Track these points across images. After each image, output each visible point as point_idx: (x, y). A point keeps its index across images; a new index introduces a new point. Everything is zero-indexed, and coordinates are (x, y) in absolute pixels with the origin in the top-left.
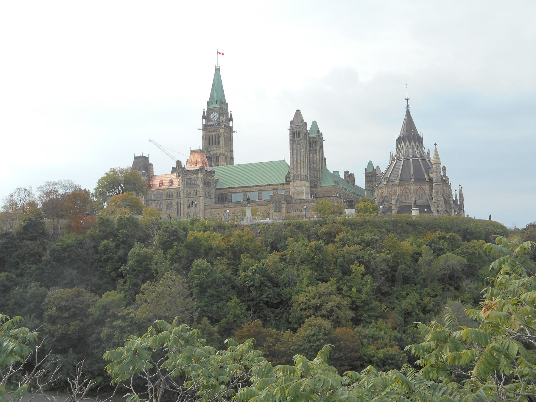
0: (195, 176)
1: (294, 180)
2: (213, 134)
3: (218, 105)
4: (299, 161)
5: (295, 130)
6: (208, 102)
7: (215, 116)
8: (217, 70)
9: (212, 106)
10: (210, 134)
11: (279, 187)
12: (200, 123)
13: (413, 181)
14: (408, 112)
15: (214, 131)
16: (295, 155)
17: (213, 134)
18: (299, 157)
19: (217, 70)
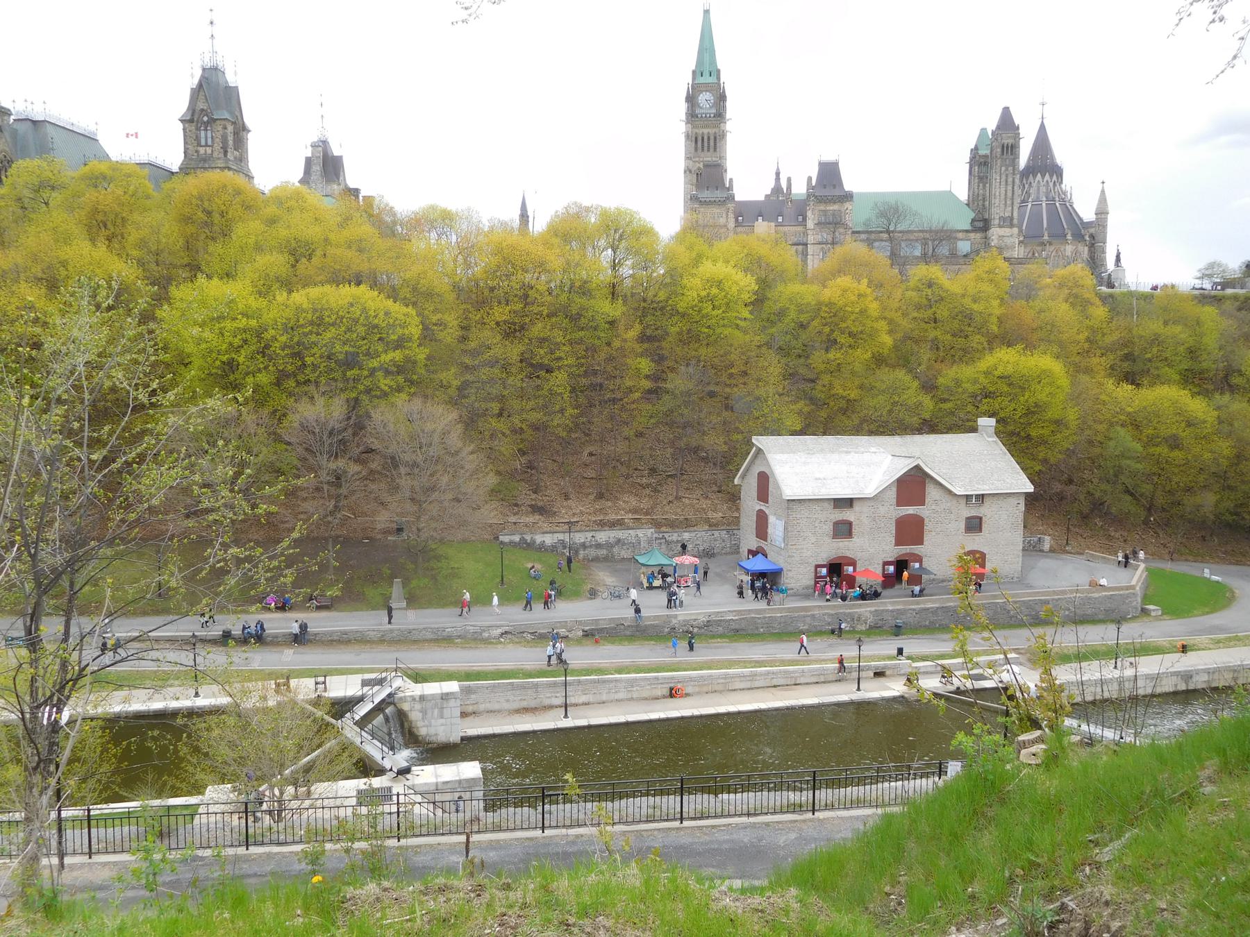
0: (836, 207)
1: (1000, 226)
2: (706, 131)
3: (712, 80)
4: (1010, 194)
5: (1006, 142)
6: (694, 72)
7: (705, 99)
8: (707, 12)
9: (701, 80)
10: (700, 131)
11: (960, 235)
12: (682, 108)
13: (1069, 237)
14: (1042, 127)
15: (706, 126)
16: (1003, 183)
17: (706, 131)
18: (1010, 188)
19: (707, 12)
